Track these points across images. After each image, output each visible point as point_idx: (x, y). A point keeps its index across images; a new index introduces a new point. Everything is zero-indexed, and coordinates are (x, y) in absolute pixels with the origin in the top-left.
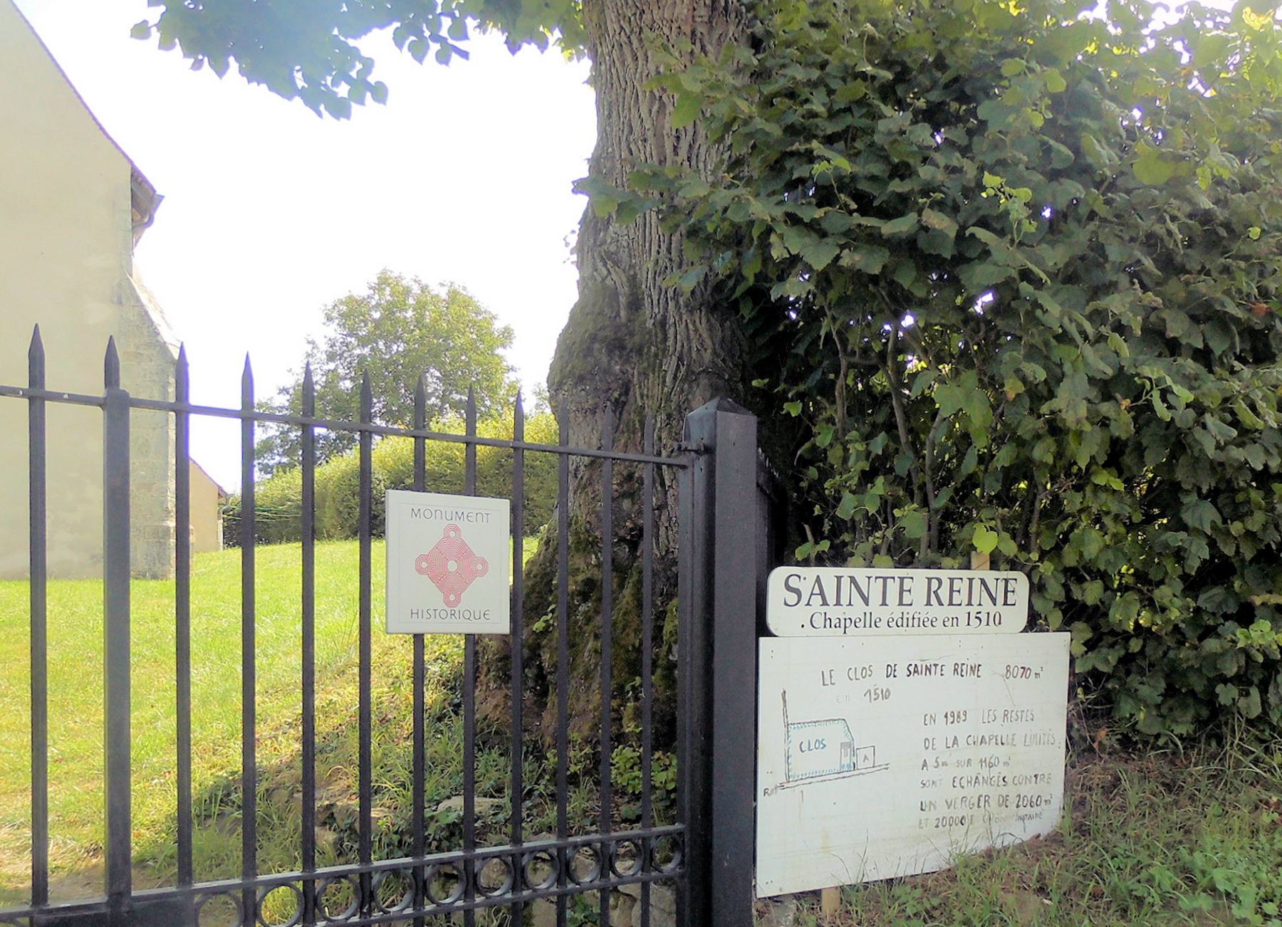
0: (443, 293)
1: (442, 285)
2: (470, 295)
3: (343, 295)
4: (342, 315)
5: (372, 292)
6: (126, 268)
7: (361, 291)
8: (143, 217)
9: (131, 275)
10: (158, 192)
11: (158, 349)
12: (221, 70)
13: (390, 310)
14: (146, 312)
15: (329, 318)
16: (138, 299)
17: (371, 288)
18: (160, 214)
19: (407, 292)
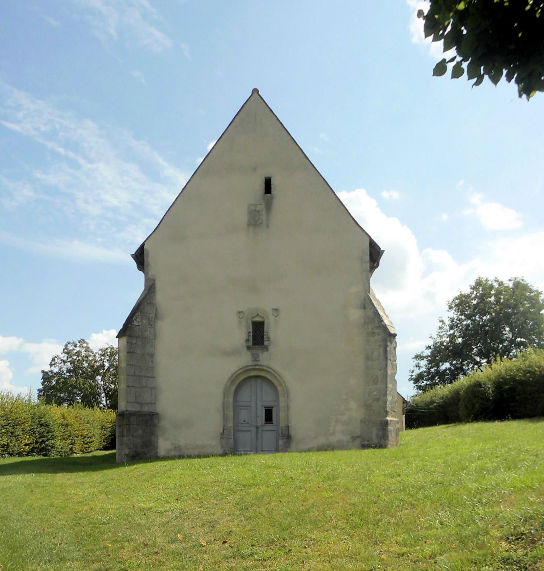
0: (511, 285)
1: (510, 280)
2: (525, 283)
3: (457, 294)
4: (457, 305)
5: (472, 290)
6: (367, 289)
7: (467, 291)
8: (374, 264)
9: (370, 293)
10: (382, 249)
11: (382, 328)
12: (495, 80)
13: (482, 298)
14: (377, 311)
15: (451, 308)
16: (373, 305)
17: (471, 289)
18: (382, 261)
19: (491, 287)
